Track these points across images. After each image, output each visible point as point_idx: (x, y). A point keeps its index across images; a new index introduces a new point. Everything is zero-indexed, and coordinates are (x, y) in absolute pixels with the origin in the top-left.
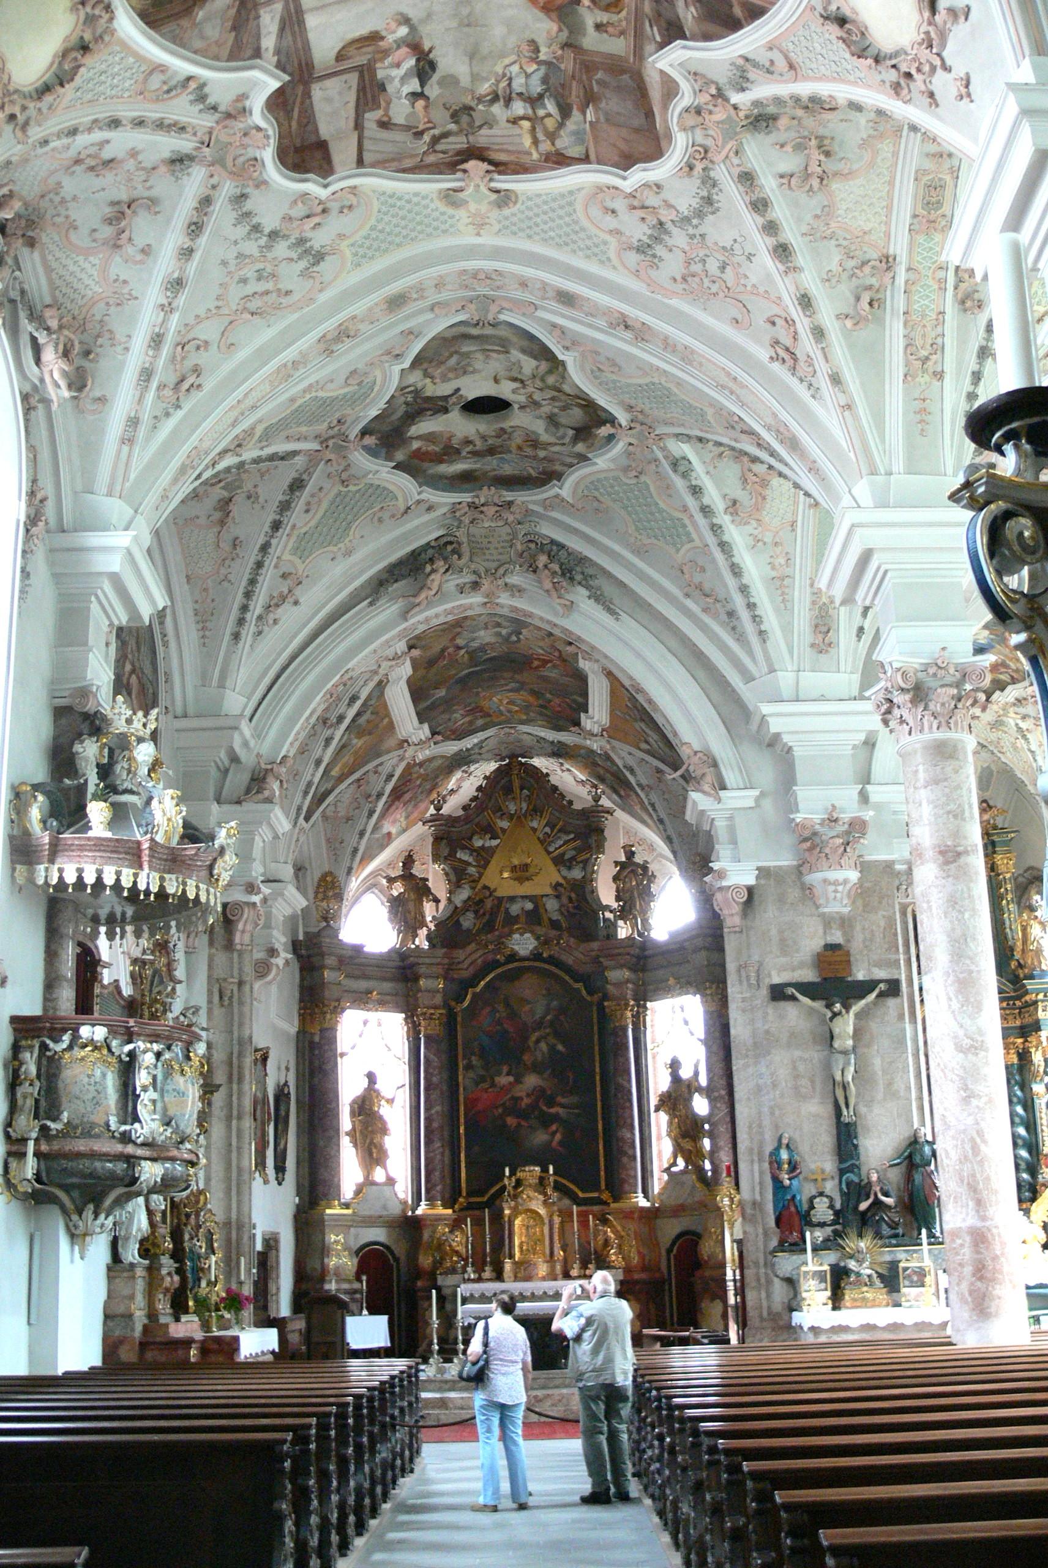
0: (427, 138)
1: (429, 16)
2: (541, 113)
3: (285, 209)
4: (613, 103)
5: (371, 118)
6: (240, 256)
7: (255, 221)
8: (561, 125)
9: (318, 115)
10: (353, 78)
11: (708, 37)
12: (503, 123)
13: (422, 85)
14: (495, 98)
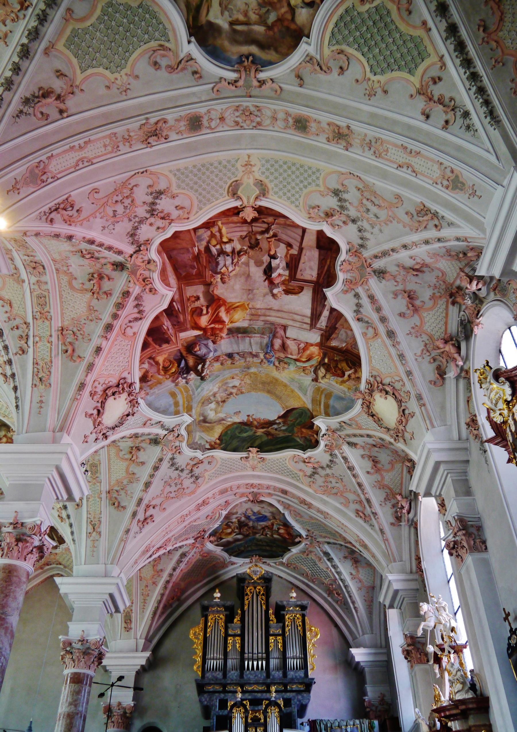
0: (271, 233)
1: (264, 296)
2: (218, 247)
3: (344, 227)
4: (186, 258)
5: (294, 251)
6: (373, 228)
7: (360, 234)
8: (209, 242)
9: (317, 263)
10: (298, 276)
11: (157, 318)
12: (235, 239)
13: (270, 262)
14: (239, 252)
